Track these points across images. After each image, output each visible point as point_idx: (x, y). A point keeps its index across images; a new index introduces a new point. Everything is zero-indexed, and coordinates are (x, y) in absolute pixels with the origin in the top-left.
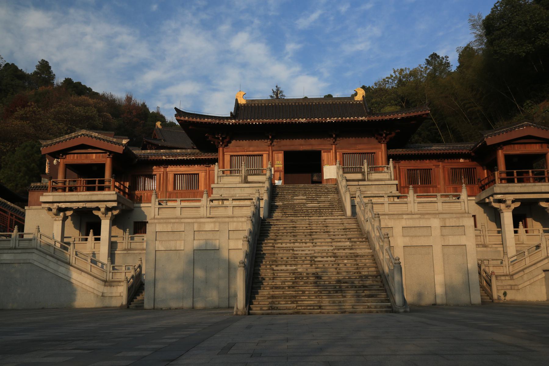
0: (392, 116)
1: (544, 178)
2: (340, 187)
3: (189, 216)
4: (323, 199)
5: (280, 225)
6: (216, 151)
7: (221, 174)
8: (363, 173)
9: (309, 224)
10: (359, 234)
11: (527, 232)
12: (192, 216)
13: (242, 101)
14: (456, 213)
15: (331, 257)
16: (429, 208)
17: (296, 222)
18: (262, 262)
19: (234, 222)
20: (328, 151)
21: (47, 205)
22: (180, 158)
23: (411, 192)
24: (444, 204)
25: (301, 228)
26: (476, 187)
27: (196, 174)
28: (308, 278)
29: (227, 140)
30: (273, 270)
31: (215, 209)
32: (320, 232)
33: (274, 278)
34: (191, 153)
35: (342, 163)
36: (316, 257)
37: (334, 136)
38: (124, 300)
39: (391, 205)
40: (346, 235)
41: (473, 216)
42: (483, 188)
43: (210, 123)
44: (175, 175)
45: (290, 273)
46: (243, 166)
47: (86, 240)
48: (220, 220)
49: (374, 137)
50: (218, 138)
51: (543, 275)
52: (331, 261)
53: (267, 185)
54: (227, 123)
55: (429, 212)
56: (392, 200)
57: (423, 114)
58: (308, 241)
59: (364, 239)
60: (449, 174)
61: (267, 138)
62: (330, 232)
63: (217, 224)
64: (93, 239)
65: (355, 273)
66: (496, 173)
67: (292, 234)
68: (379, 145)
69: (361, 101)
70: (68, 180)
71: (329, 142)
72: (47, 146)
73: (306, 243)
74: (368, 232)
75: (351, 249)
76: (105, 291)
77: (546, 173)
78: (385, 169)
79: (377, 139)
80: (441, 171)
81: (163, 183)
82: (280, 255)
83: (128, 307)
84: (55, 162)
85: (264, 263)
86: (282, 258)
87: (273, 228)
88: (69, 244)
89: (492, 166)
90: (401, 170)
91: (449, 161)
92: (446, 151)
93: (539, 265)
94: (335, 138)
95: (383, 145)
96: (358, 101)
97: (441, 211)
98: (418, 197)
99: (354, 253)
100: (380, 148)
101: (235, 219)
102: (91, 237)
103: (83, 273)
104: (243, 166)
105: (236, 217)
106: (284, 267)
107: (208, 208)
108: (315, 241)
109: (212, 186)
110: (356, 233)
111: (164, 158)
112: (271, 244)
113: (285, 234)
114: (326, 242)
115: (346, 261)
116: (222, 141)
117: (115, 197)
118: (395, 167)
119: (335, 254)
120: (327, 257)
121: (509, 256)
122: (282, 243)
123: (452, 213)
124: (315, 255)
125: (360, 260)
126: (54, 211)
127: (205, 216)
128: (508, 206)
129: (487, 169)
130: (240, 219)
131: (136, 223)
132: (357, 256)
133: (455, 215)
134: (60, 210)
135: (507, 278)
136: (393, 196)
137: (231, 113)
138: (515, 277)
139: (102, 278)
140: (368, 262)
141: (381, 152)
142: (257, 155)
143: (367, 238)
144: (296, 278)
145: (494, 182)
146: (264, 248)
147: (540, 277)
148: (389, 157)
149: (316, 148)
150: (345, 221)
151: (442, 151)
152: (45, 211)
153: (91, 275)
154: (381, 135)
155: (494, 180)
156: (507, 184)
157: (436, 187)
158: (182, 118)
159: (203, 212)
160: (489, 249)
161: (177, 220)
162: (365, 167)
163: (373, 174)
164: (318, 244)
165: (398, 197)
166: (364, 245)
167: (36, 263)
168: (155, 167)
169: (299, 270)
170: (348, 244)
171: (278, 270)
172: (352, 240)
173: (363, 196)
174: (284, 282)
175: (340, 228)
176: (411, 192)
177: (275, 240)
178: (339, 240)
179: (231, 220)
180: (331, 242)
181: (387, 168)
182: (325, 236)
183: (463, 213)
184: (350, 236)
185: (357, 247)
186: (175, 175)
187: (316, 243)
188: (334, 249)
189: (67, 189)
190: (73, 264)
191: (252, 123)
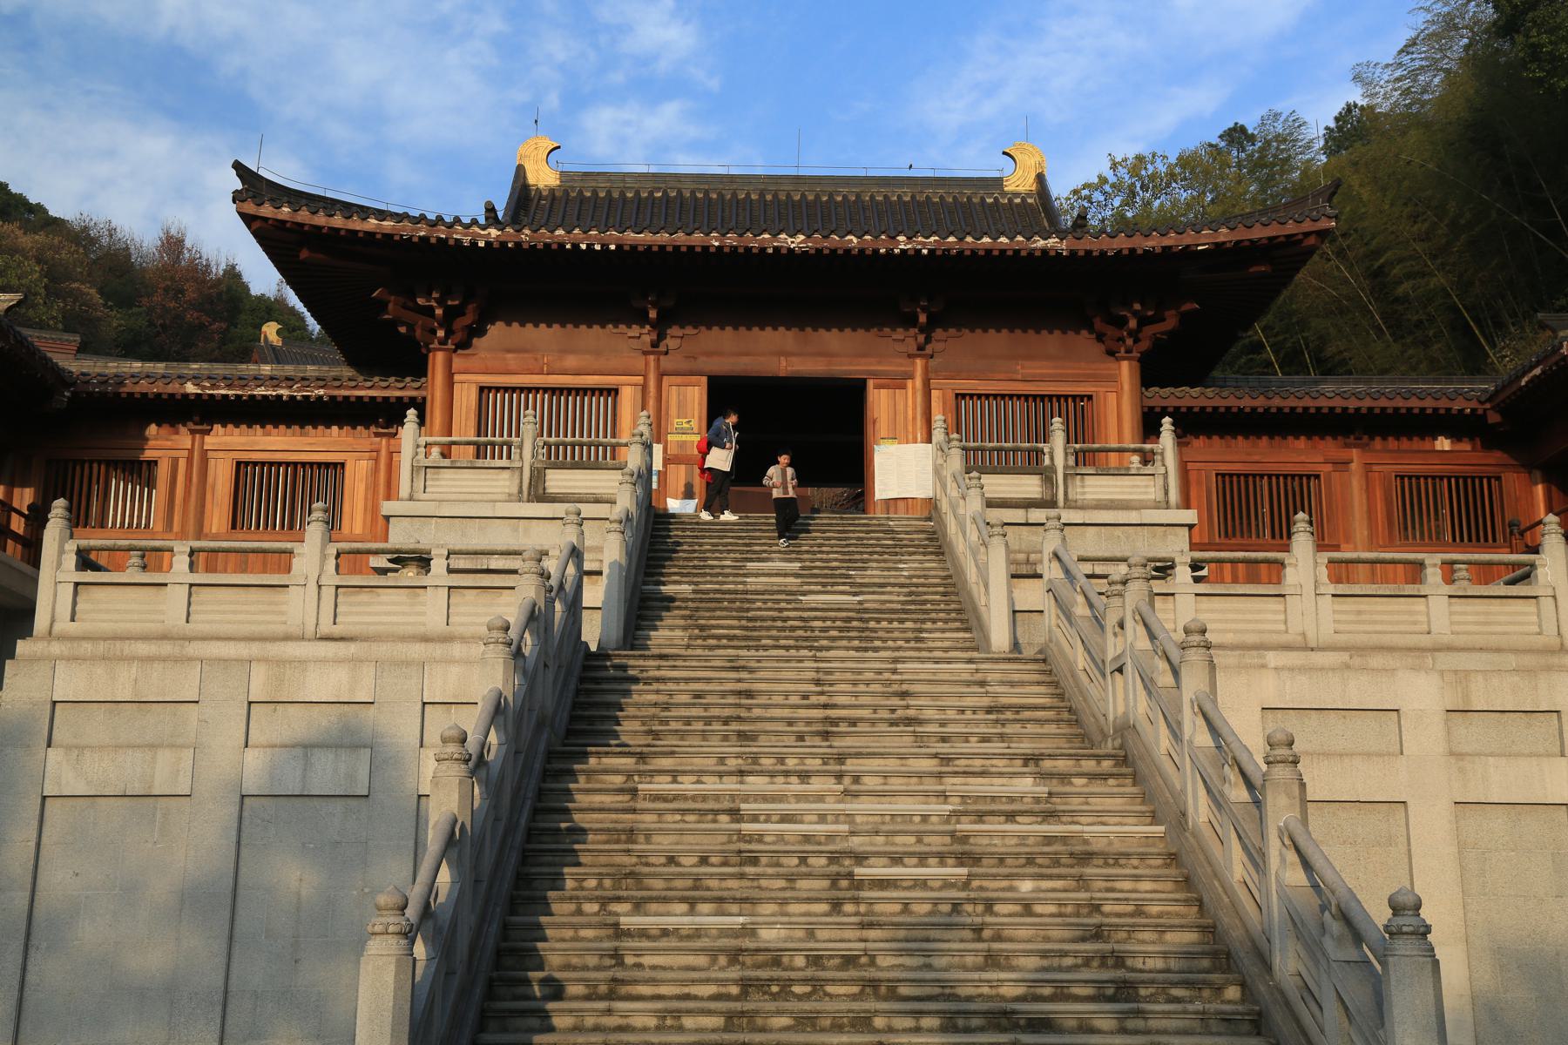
0: (1171, 240)
2: (952, 528)
4: (873, 574)
5: (676, 680)
6: (419, 369)
8: (1047, 476)
9: (818, 682)
10: (1069, 738)
12: (246, 629)
13: (543, 177)
14: (1516, 651)
15: (942, 857)
16: (1387, 617)
17: (751, 671)
18: (556, 881)
19: (451, 661)
20: (897, 382)
22: (260, 391)
24: (1459, 605)
27: (335, 465)
28: (817, 985)
29: (468, 319)
30: (619, 932)
31: (364, 597)
32: (873, 722)
36: (860, 858)
37: (923, 318)
40: (1002, 737)
43: (388, 237)
44: (239, 464)
45: (713, 953)
46: (528, 428)
48: (383, 650)
49: (1091, 329)
50: (432, 309)
52: (947, 885)
53: (626, 501)
54: (466, 241)
55: (1387, 640)
57: (1307, 234)
58: (814, 764)
59: (1107, 765)
60: (1388, 503)
61: (642, 319)
62: (920, 722)
63: (368, 672)
65: (1087, 963)
67: (734, 726)
68: (1111, 364)
69: (1029, 194)
71: (900, 347)
73: (804, 776)
75: (1050, 815)
79: (1100, 338)
80: (1356, 484)
82: (664, 842)
85: (569, 884)
86: (672, 860)
87: (642, 695)
90: (1193, 476)
91: (1392, 443)
94: (927, 330)
95: (1125, 365)
96: (1017, 195)
97: (1447, 639)
99: (1064, 839)
100: (1113, 379)
101: (457, 650)
104: (528, 428)
105: (464, 639)
106: (677, 917)
107: (328, 593)
108: (851, 765)
109: (388, 507)
110: (1051, 729)
111: (190, 388)
112: (618, 780)
113: (699, 726)
115: (1026, 886)
116: (447, 322)
119: (964, 839)
120: (922, 859)
122: (674, 774)
123: (1498, 650)
124: (856, 842)
125: (1108, 878)
127: (310, 629)
129: (1548, 480)
132: (1086, 857)
133: (1512, 660)
140: (1152, 890)
141: (1118, 395)
142: (593, 391)
143: (1123, 759)
144: (746, 985)
146: (582, 800)
150: (994, 673)
154: (1121, 323)
158: (267, 211)
161: (167, 648)
162: (1057, 448)
163: (1089, 480)
164: (870, 783)
166: (1114, 796)
168: (152, 429)
169: (769, 936)
170: (1026, 785)
171: (643, 934)
172: (1047, 764)
174: (677, 1014)
175: (968, 702)
177: (642, 757)
178: (977, 764)
179: (438, 650)
180: (939, 776)
182: (901, 740)
183: (1547, 651)
184: (1026, 747)
185: (1075, 803)
186: (239, 464)
187: (857, 779)
188: (956, 814)
191: (576, 246)
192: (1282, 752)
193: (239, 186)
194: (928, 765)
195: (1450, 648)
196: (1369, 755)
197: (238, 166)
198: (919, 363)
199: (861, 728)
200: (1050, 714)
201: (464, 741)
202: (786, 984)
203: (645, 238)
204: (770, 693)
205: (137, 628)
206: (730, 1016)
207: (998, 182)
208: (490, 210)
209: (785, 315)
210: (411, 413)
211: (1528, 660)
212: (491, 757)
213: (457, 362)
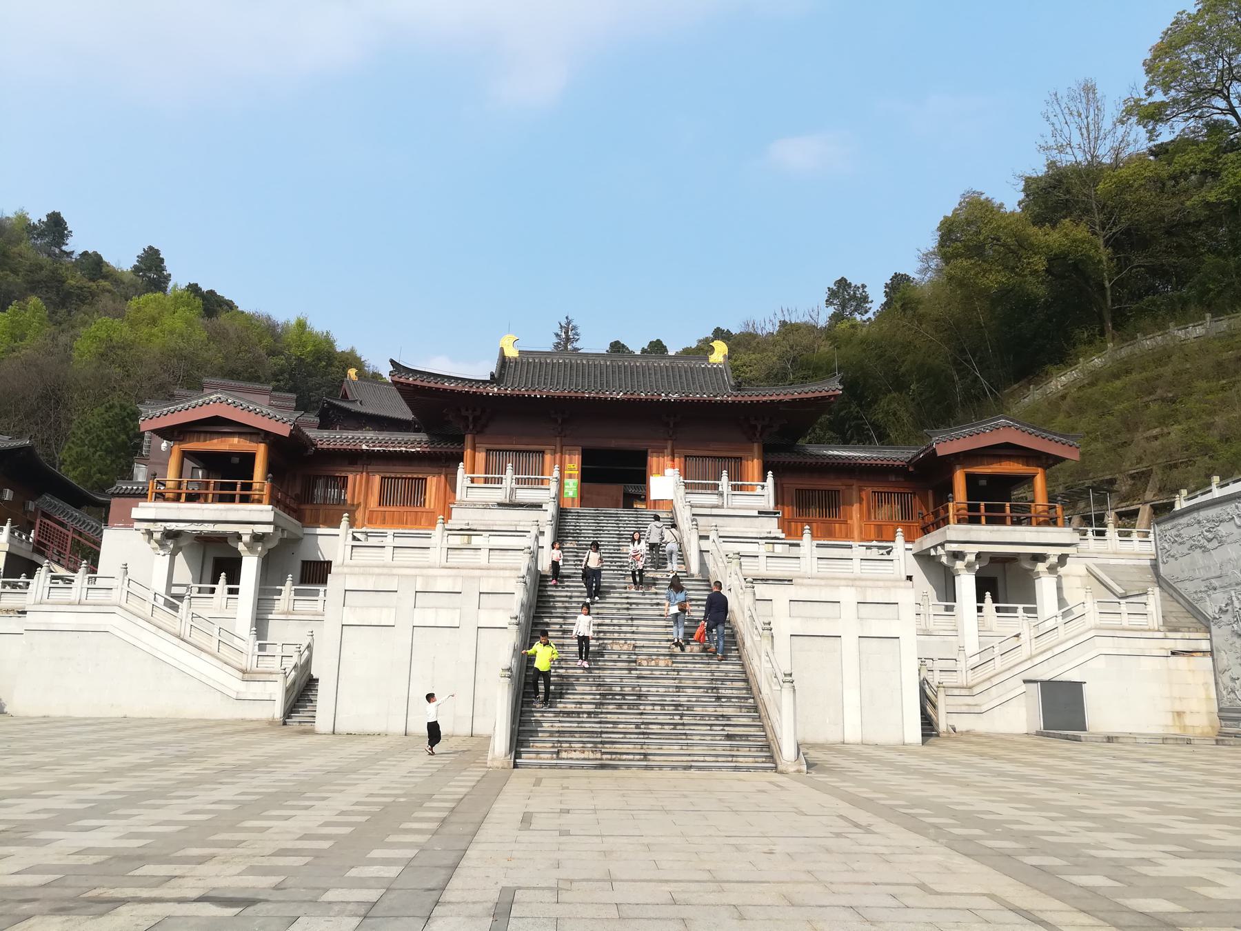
3: (407, 564)
6: (461, 440)
11: (998, 610)
12: (414, 564)
13: (511, 353)
16: (838, 568)
21: (145, 525)
23: (807, 536)
24: (864, 563)
31: (457, 552)
38: (277, 711)
42: (926, 530)
46: (509, 471)
47: (213, 591)
50: (467, 418)
51: (1024, 687)
63: (460, 581)
64: (226, 591)
66: (951, 505)
78: (758, 490)
83: (285, 723)
88: (180, 597)
98: (818, 546)
102: (222, 586)
103: (203, 655)
104: (509, 471)
111: (364, 447)
121: (969, 652)
126: (157, 536)
130: (501, 573)
131: (305, 564)
133: (881, 584)
134: (170, 535)
135: (964, 692)
137: (492, 375)
138: (976, 690)
145: (946, 521)
149: (639, 445)
152: (140, 538)
153: (218, 658)
155: (948, 517)
156: (969, 526)
157: (845, 522)
159: (436, 555)
161: (385, 571)
179: (485, 573)
181: (763, 487)
183: (897, 581)
189: (184, 496)
193: (391, 369)
195: (860, 579)
197: (392, 362)
198: (670, 443)
205: (374, 563)
211: (889, 584)
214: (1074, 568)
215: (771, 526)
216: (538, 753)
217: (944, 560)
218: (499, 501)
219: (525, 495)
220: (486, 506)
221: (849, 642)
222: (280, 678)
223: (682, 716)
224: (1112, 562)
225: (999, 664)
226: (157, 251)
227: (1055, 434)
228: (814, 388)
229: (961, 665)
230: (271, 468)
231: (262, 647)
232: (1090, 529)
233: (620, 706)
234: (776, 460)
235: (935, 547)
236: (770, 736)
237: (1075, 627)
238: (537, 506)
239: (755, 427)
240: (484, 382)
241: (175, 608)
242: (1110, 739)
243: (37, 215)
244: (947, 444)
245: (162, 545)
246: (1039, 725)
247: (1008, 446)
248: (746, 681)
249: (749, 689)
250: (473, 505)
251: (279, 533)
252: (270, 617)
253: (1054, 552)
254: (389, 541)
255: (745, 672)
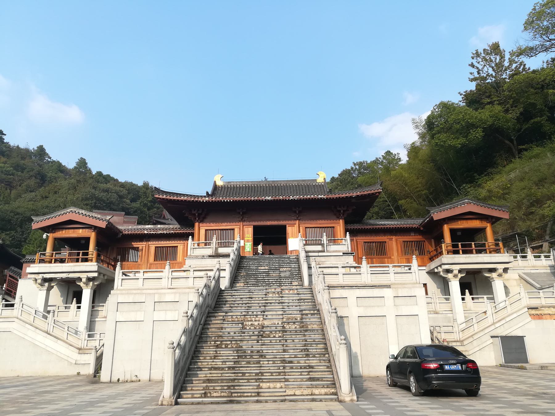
1: (486, 250)
3: (150, 287)
5: (237, 295)
6: (193, 226)
7: (196, 246)
8: (322, 245)
9: (266, 295)
11: (473, 299)
12: (154, 287)
13: (220, 183)
17: (253, 293)
20: (293, 225)
21: (33, 276)
25: (257, 299)
26: (426, 257)
28: (251, 356)
29: (203, 216)
31: (177, 280)
32: (275, 303)
33: (215, 357)
34: (173, 227)
35: (305, 236)
39: (345, 276)
41: (424, 284)
42: (431, 259)
46: (214, 239)
50: (195, 214)
51: (491, 340)
56: (349, 271)
57: (376, 193)
59: (316, 312)
63: (178, 295)
66: (443, 245)
67: (248, 305)
70: (54, 252)
72: (38, 222)
74: (320, 304)
76: (78, 359)
77: (487, 245)
81: (145, 255)
82: (228, 330)
84: (44, 236)
88: (49, 312)
89: (439, 239)
90: (358, 243)
92: (398, 226)
93: (486, 331)
95: (341, 220)
100: (339, 223)
102: (74, 305)
104: (214, 239)
107: (170, 279)
108: (266, 313)
110: (310, 304)
111: (146, 232)
113: (240, 305)
114: (277, 315)
117: (95, 268)
118: (352, 240)
121: (459, 322)
125: (309, 335)
127: (166, 287)
128: (455, 276)
134: (45, 280)
136: (350, 267)
138: (465, 343)
139: (78, 346)
141: (340, 226)
143: (318, 310)
145: (441, 253)
147: (489, 342)
148: (346, 230)
151: (395, 226)
152: (32, 282)
155: (442, 251)
156: (454, 256)
157: (390, 258)
159: (164, 283)
160: (440, 315)
161: (139, 291)
162: (325, 239)
164: (269, 317)
165: (355, 267)
167: (15, 332)
172: (304, 312)
173: (318, 266)
175: (295, 298)
176: (364, 262)
177: (226, 313)
180: (282, 315)
184: (303, 308)
190: (51, 333)
192: (334, 311)
194: (281, 313)
196: (378, 306)
198: (297, 221)
199: (273, 304)
200: (310, 301)
201: (187, 313)
202: (246, 356)
203: (238, 199)
204: (255, 298)
206: (235, 362)
207: (316, 180)
208: (207, 193)
209: (267, 214)
210: (190, 237)
211: (410, 286)
212: (194, 315)
213: (201, 225)
214: (512, 275)
215: (350, 260)
216: (193, 394)
217: (442, 274)
218: (209, 254)
219: (222, 250)
220: (203, 257)
221: (391, 320)
222: (94, 351)
223: (284, 367)
224: (532, 271)
225: (476, 328)
226: (85, 159)
227: (495, 206)
228: (367, 190)
229: (456, 329)
230: (99, 245)
231: (89, 336)
232: (518, 255)
233: (248, 363)
234: (352, 227)
235: (437, 268)
236: (335, 377)
237: (516, 306)
238: (228, 256)
239: (340, 211)
240: (205, 196)
241: (45, 317)
242: (543, 367)
243: (33, 146)
244: (438, 214)
245: (42, 285)
246: (502, 361)
247: (470, 213)
248: (326, 344)
249: (326, 349)
250: (197, 257)
251: (102, 276)
252: (97, 319)
253: (501, 267)
254: (140, 275)
255: (325, 339)
